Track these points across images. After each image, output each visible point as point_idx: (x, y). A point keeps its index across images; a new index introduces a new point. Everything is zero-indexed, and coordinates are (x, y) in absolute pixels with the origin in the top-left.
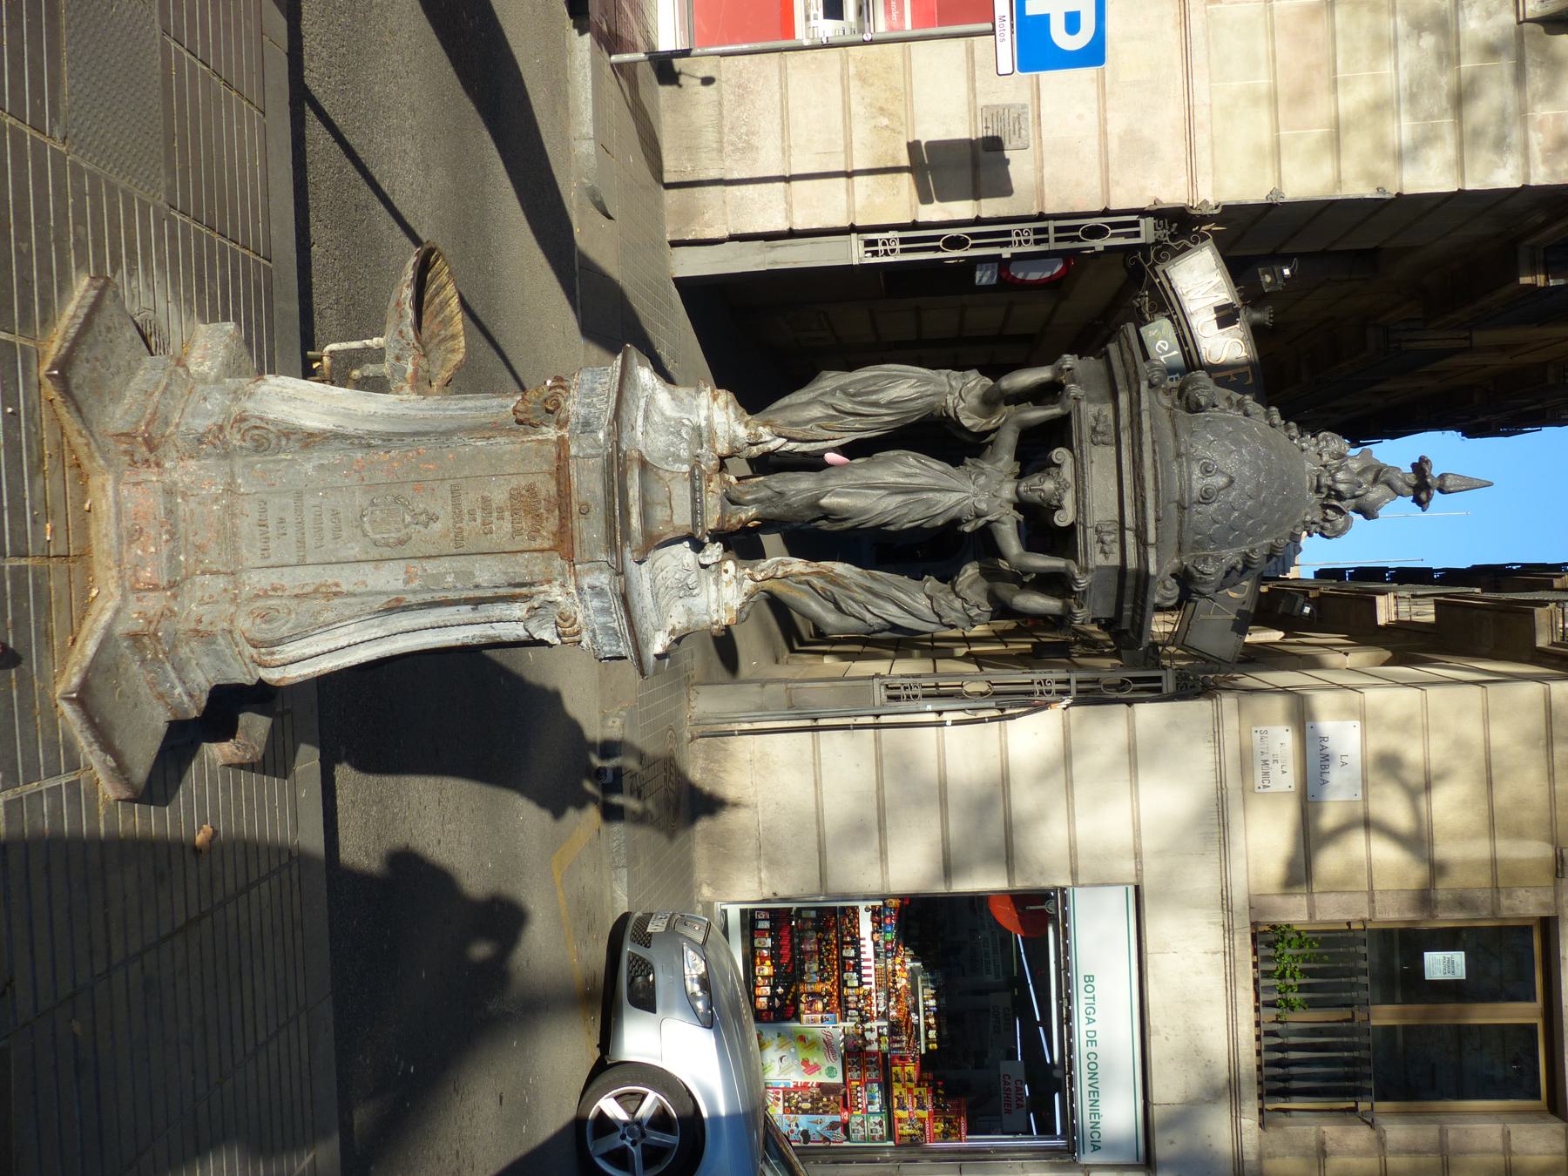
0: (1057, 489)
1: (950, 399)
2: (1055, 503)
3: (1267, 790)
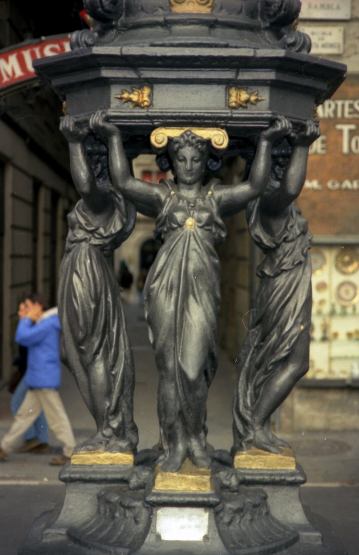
0: (191, 145)
1: (97, 242)
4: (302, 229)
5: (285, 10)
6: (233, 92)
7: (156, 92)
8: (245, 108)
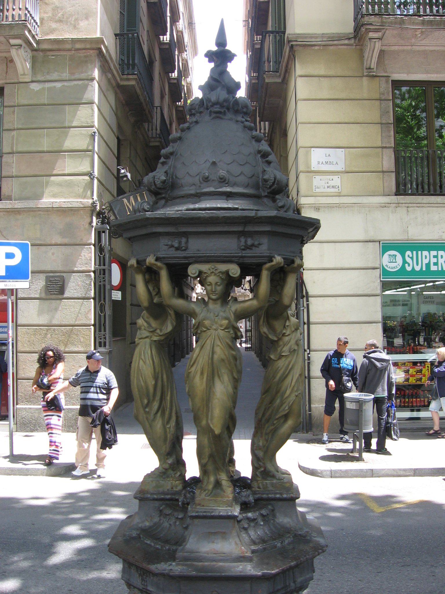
0: (215, 275)
1: (155, 338)
2: (224, 277)
3: (340, 187)
4: (296, 327)
5: (278, 184)
6: (243, 240)
7: (190, 240)
8: (251, 249)
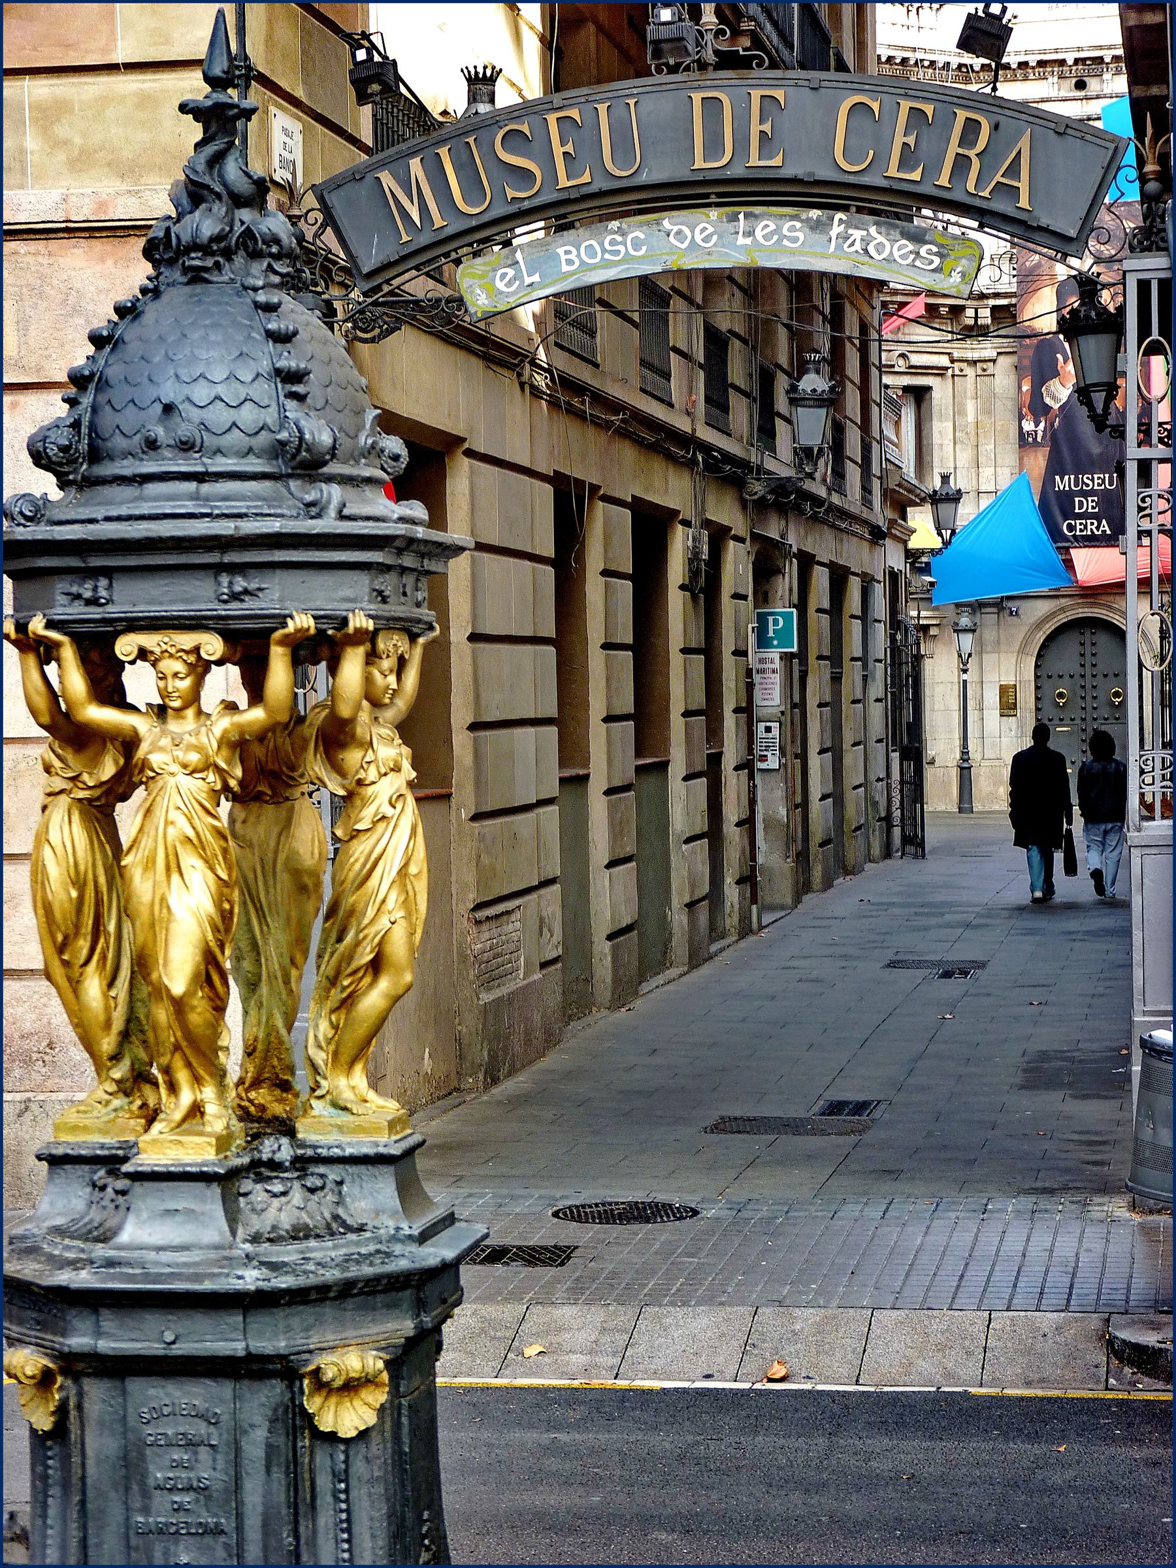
0: (171, 656)
1: (82, 794)
6: (225, 579)
8: (242, 601)
